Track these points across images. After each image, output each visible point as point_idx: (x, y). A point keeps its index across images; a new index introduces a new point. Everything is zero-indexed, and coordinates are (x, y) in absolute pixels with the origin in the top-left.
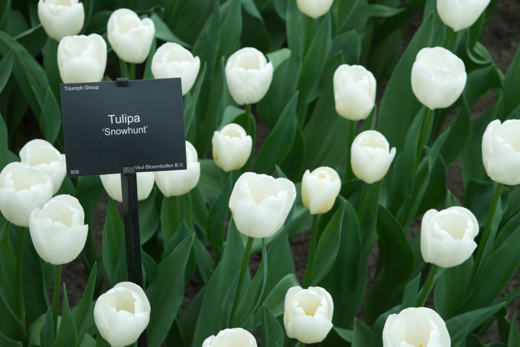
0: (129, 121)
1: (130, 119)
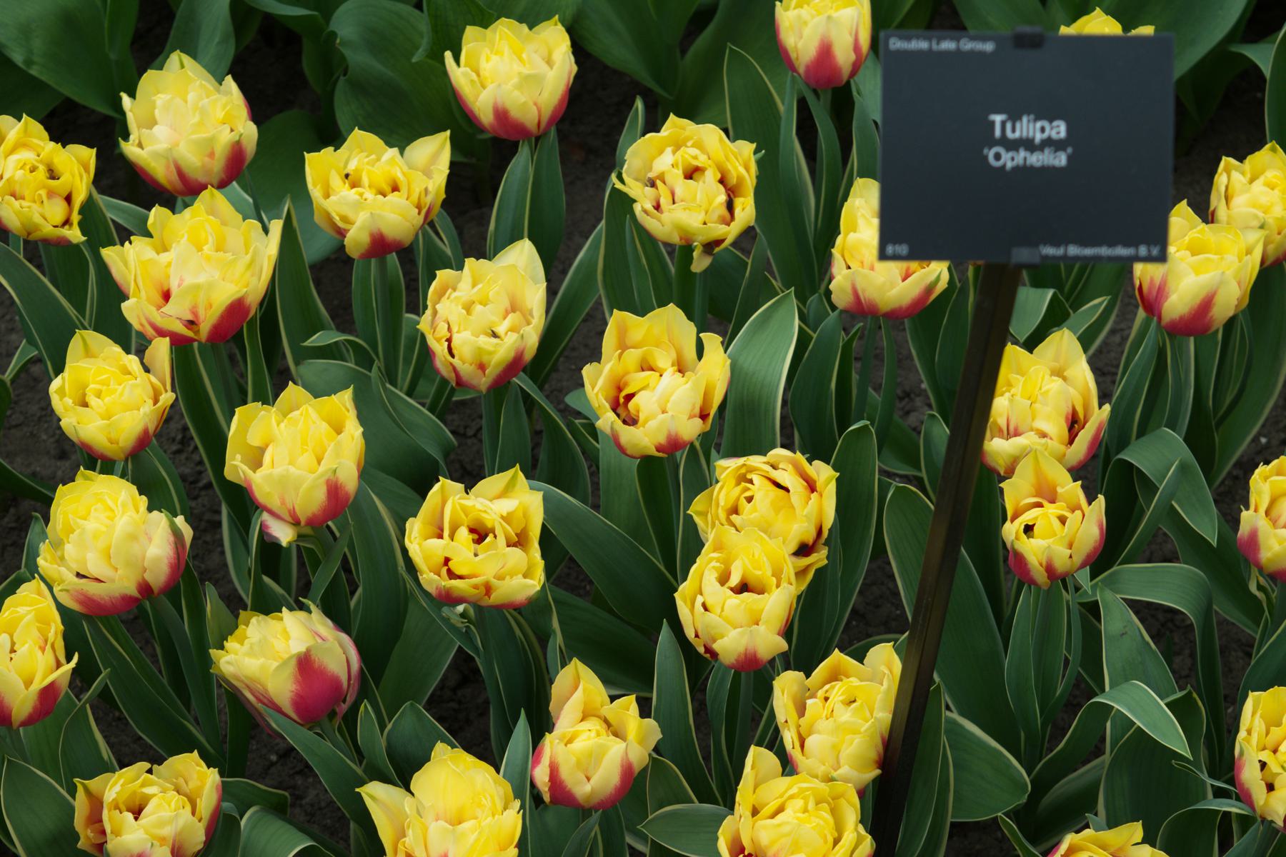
1: (1043, 130)
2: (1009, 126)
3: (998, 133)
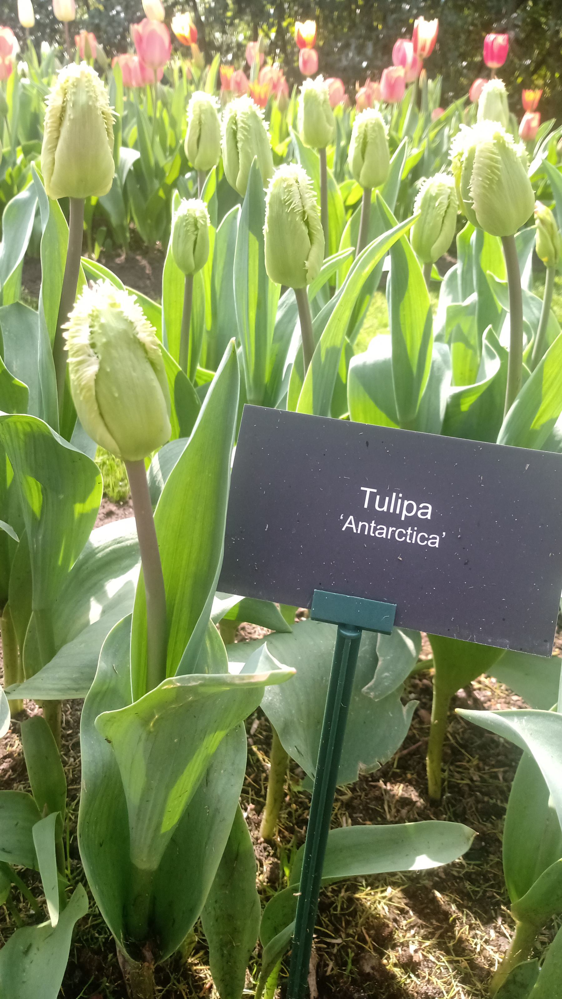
1: (410, 508)
2: (378, 497)
3: (366, 506)
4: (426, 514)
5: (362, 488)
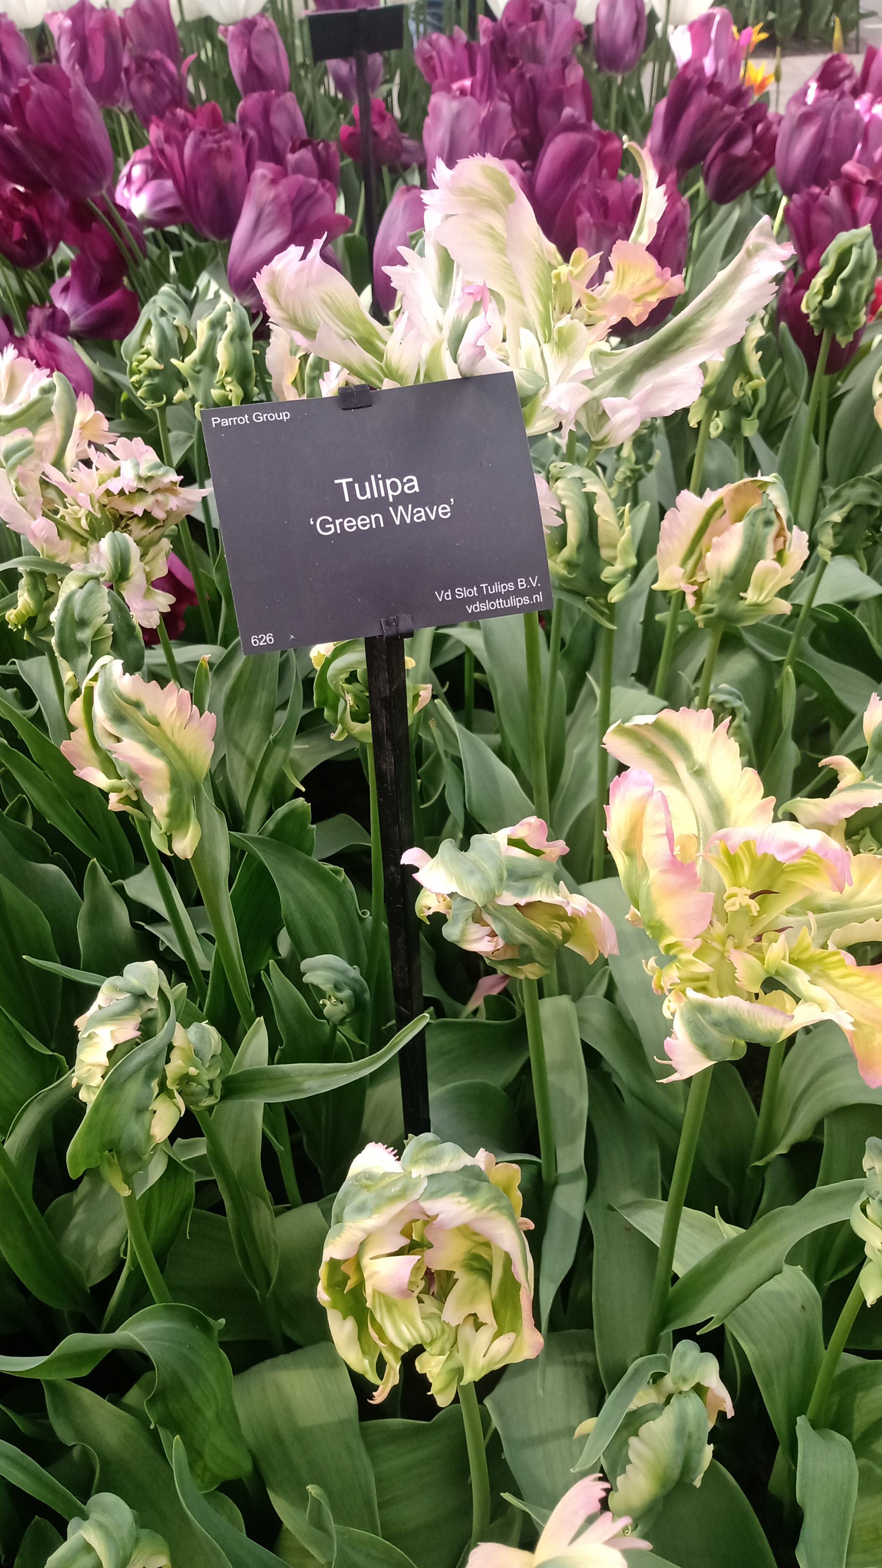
0: (390, 493)
1: (394, 487)
2: (356, 485)
3: (347, 500)
4: (413, 486)
5: (336, 482)
